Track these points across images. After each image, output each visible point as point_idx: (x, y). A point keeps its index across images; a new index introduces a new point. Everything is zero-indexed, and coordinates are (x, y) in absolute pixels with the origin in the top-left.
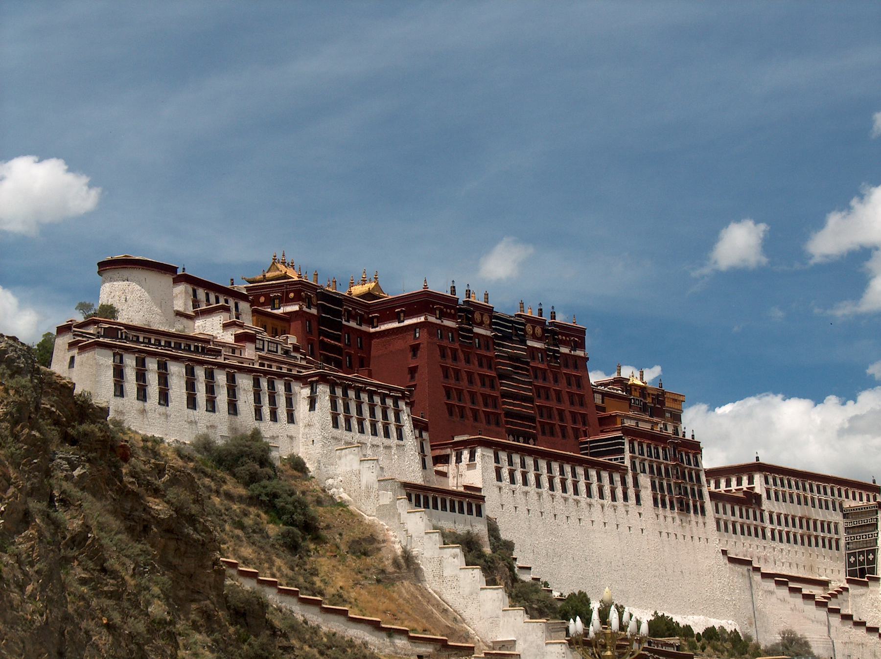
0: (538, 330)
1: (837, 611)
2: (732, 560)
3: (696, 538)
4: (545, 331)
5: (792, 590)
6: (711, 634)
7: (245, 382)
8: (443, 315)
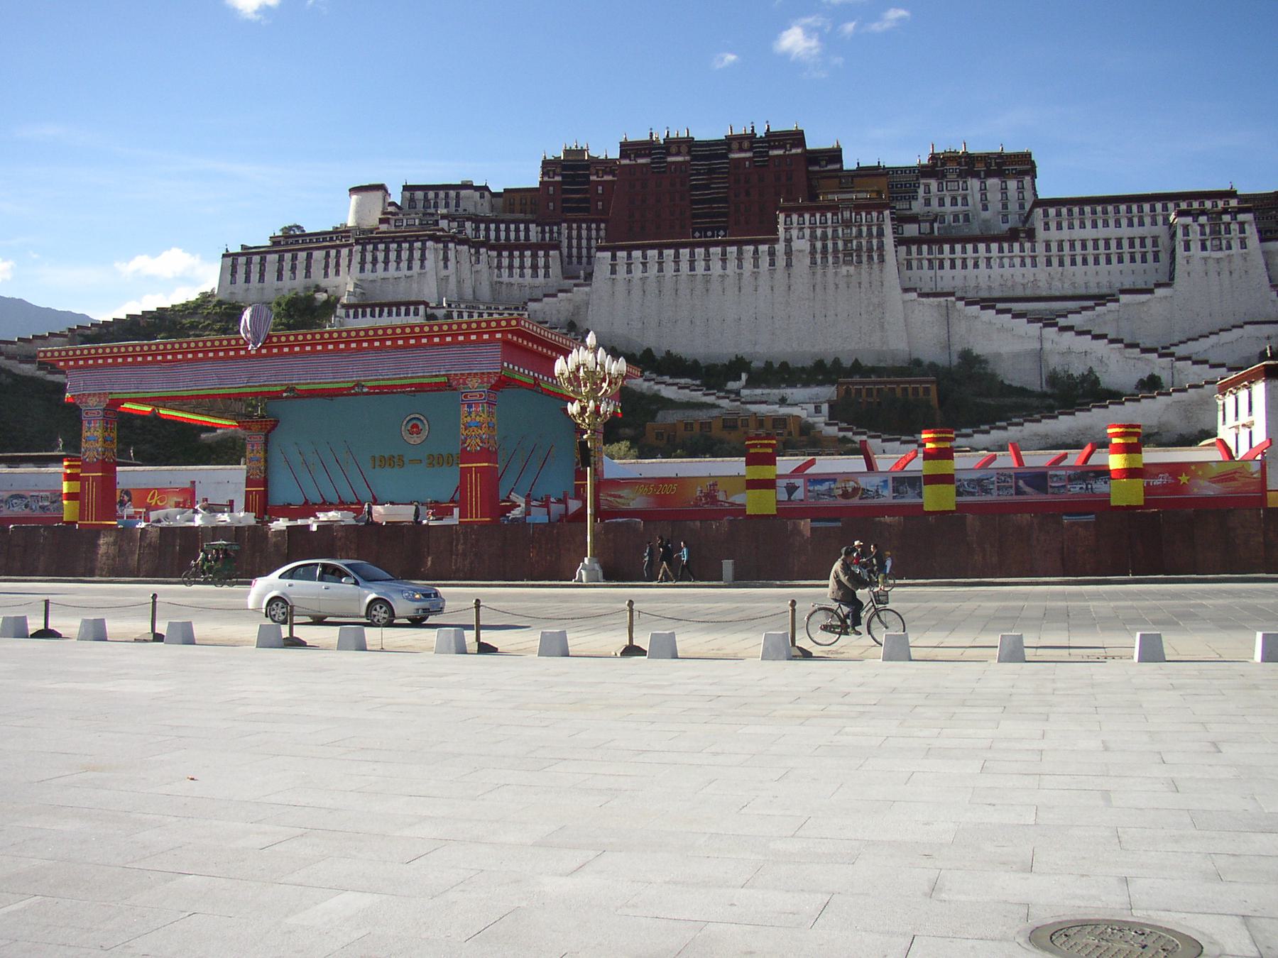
0: (746, 144)
1: (1055, 325)
2: (921, 295)
4: (752, 143)
5: (999, 312)
6: (819, 365)
7: (318, 255)
8: (638, 156)
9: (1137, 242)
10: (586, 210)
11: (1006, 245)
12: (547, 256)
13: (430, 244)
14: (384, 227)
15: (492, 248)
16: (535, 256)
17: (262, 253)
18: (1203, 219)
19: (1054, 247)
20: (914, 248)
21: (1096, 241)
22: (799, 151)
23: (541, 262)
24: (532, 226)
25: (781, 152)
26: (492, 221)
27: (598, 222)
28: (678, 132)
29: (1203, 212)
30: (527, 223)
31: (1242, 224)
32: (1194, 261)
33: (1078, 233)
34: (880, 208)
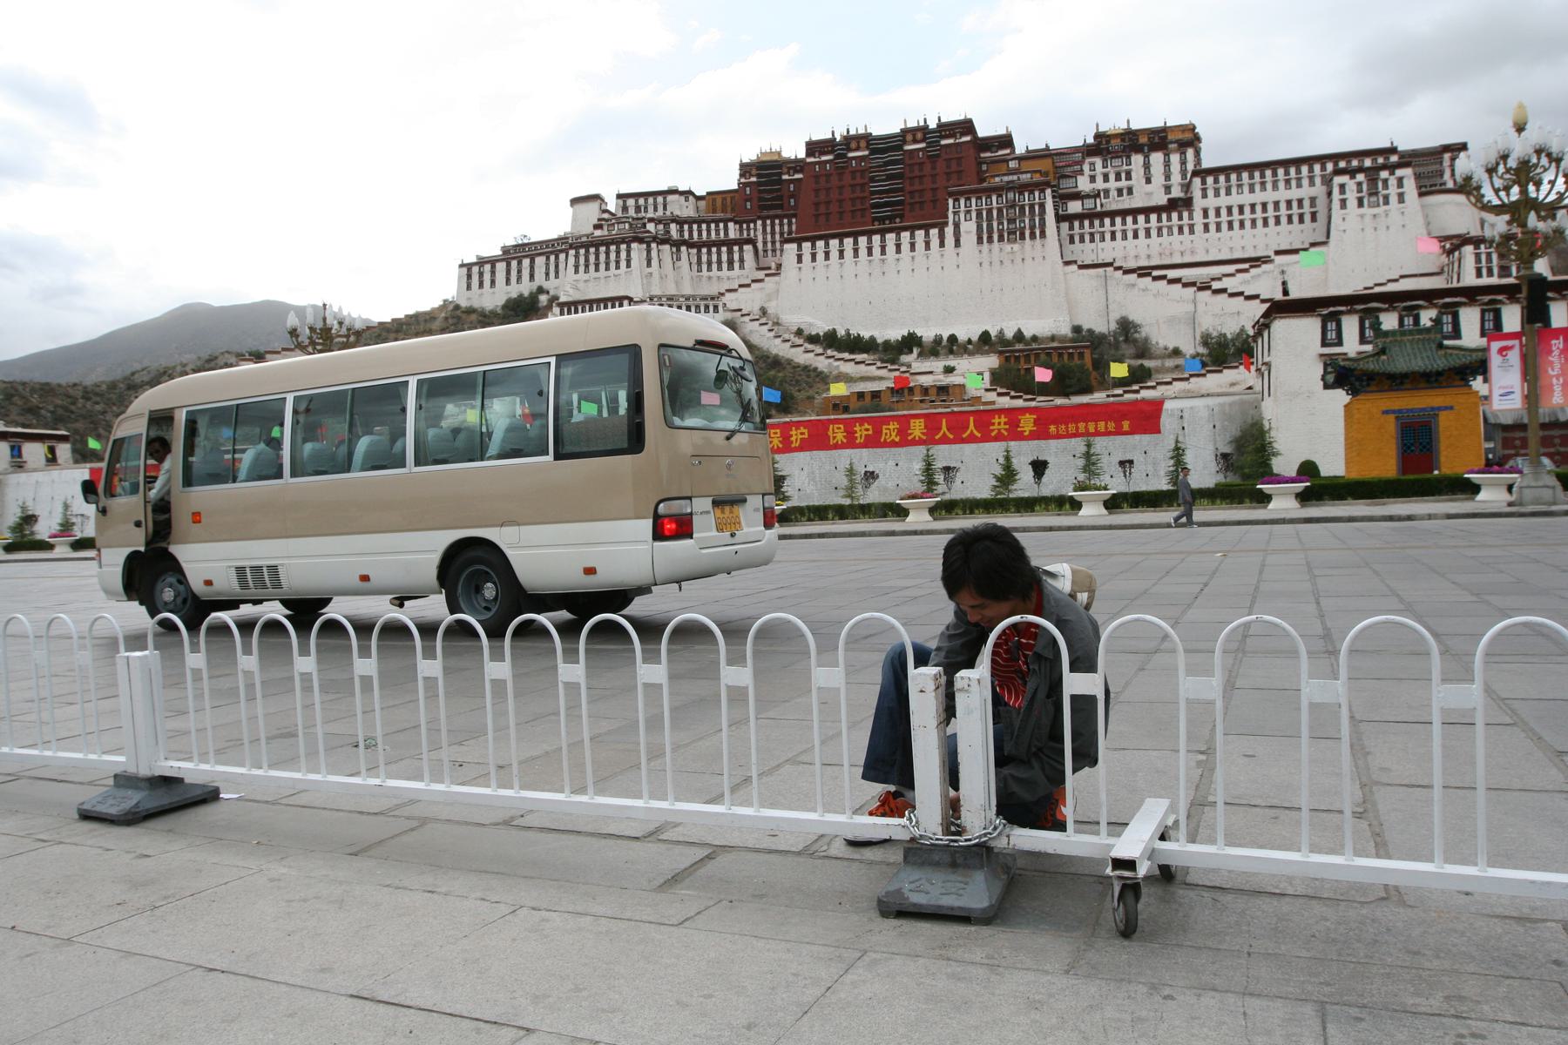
0: (919, 136)
1: (1209, 288)
2: (1082, 267)
3: (1028, 261)
5: (1156, 279)
6: (985, 337)
7: (540, 261)
9: (1295, 205)
10: (781, 207)
11: (1164, 216)
12: (741, 250)
13: (634, 245)
14: (598, 233)
15: (690, 245)
16: (730, 252)
17: (493, 262)
18: (1360, 177)
19: (1212, 213)
20: (1076, 224)
21: (1253, 206)
22: (968, 138)
23: (736, 257)
24: (731, 225)
25: (951, 141)
26: (695, 222)
27: (789, 217)
28: (857, 128)
29: (1360, 170)
30: (726, 222)
31: (1400, 181)
32: (1350, 221)
33: (1235, 199)
34: (1042, 186)
